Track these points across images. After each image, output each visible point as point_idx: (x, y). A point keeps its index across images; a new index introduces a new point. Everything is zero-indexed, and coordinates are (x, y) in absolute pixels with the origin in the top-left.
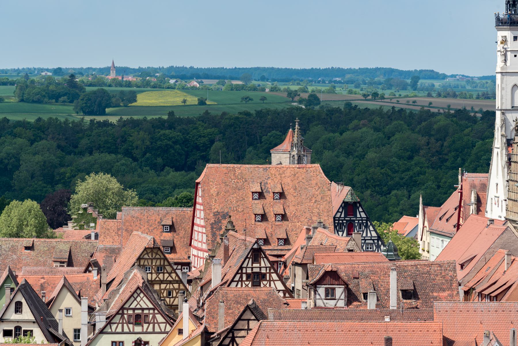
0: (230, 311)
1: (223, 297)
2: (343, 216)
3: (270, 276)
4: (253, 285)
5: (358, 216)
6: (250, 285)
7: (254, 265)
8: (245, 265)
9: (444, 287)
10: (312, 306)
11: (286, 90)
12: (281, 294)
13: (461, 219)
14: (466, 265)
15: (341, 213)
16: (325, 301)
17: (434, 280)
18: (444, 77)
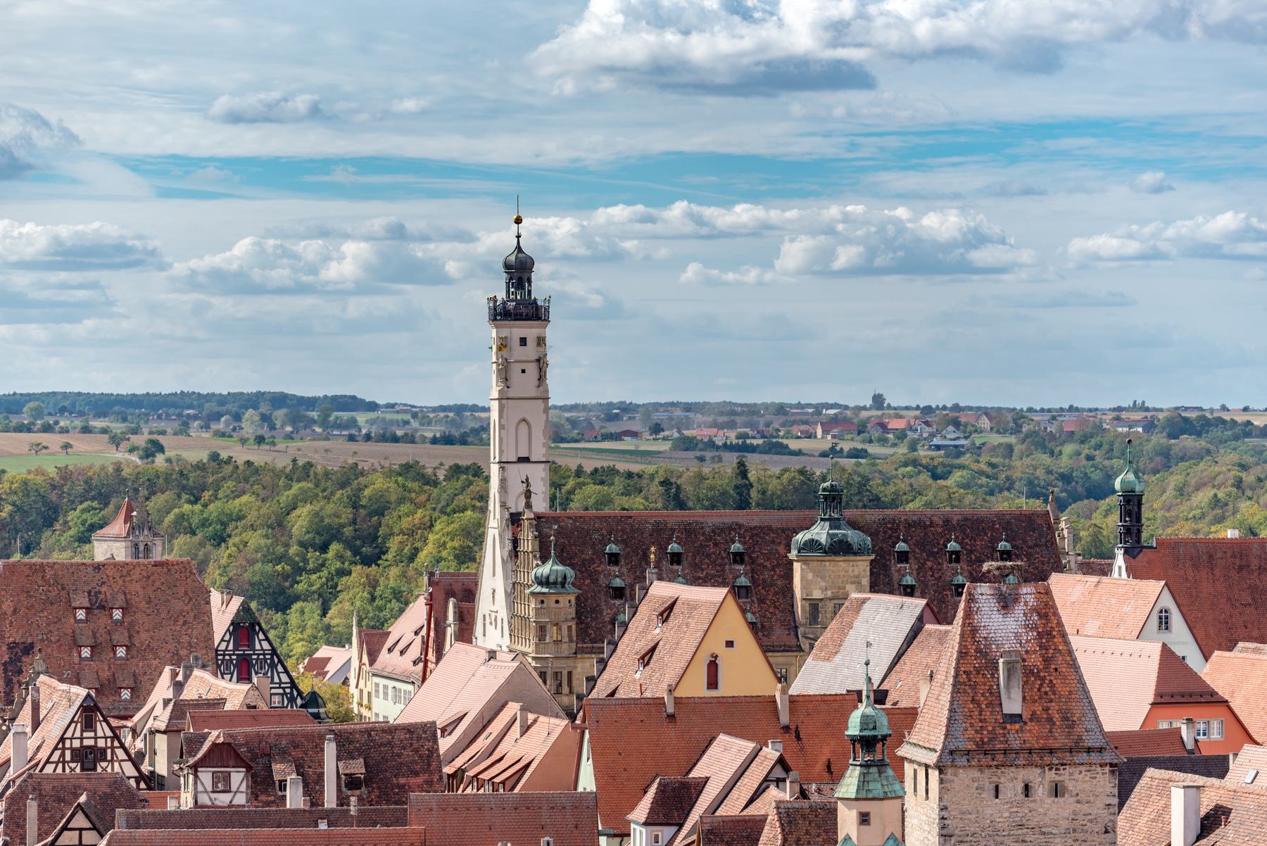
0: (47, 815)
1: (34, 789)
2: (231, 647)
3: (113, 753)
4: (83, 769)
5: (258, 647)
6: (78, 770)
7: (85, 734)
8: (69, 734)
9: (417, 768)
10: (191, 804)
11: (104, 431)
12: (132, 782)
13: (430, 650)
14: (449, 729)
15: (228, 642)
16: (213, 796)
17: (399, 755)
18: (373, 406)
